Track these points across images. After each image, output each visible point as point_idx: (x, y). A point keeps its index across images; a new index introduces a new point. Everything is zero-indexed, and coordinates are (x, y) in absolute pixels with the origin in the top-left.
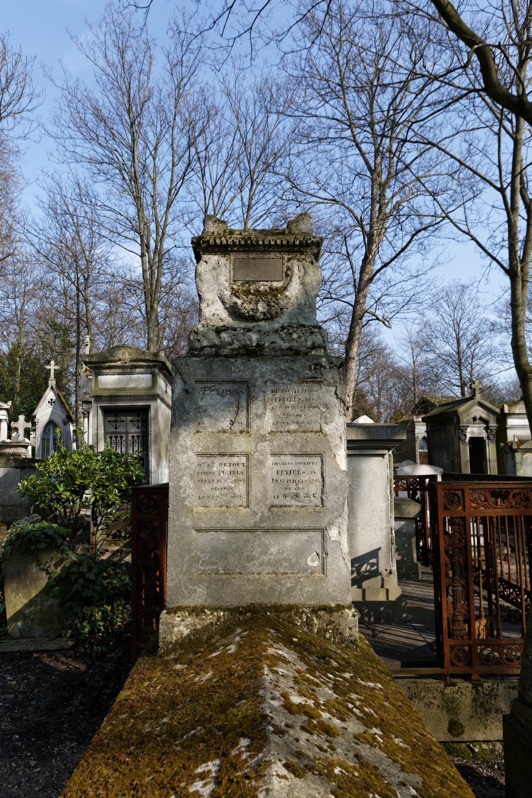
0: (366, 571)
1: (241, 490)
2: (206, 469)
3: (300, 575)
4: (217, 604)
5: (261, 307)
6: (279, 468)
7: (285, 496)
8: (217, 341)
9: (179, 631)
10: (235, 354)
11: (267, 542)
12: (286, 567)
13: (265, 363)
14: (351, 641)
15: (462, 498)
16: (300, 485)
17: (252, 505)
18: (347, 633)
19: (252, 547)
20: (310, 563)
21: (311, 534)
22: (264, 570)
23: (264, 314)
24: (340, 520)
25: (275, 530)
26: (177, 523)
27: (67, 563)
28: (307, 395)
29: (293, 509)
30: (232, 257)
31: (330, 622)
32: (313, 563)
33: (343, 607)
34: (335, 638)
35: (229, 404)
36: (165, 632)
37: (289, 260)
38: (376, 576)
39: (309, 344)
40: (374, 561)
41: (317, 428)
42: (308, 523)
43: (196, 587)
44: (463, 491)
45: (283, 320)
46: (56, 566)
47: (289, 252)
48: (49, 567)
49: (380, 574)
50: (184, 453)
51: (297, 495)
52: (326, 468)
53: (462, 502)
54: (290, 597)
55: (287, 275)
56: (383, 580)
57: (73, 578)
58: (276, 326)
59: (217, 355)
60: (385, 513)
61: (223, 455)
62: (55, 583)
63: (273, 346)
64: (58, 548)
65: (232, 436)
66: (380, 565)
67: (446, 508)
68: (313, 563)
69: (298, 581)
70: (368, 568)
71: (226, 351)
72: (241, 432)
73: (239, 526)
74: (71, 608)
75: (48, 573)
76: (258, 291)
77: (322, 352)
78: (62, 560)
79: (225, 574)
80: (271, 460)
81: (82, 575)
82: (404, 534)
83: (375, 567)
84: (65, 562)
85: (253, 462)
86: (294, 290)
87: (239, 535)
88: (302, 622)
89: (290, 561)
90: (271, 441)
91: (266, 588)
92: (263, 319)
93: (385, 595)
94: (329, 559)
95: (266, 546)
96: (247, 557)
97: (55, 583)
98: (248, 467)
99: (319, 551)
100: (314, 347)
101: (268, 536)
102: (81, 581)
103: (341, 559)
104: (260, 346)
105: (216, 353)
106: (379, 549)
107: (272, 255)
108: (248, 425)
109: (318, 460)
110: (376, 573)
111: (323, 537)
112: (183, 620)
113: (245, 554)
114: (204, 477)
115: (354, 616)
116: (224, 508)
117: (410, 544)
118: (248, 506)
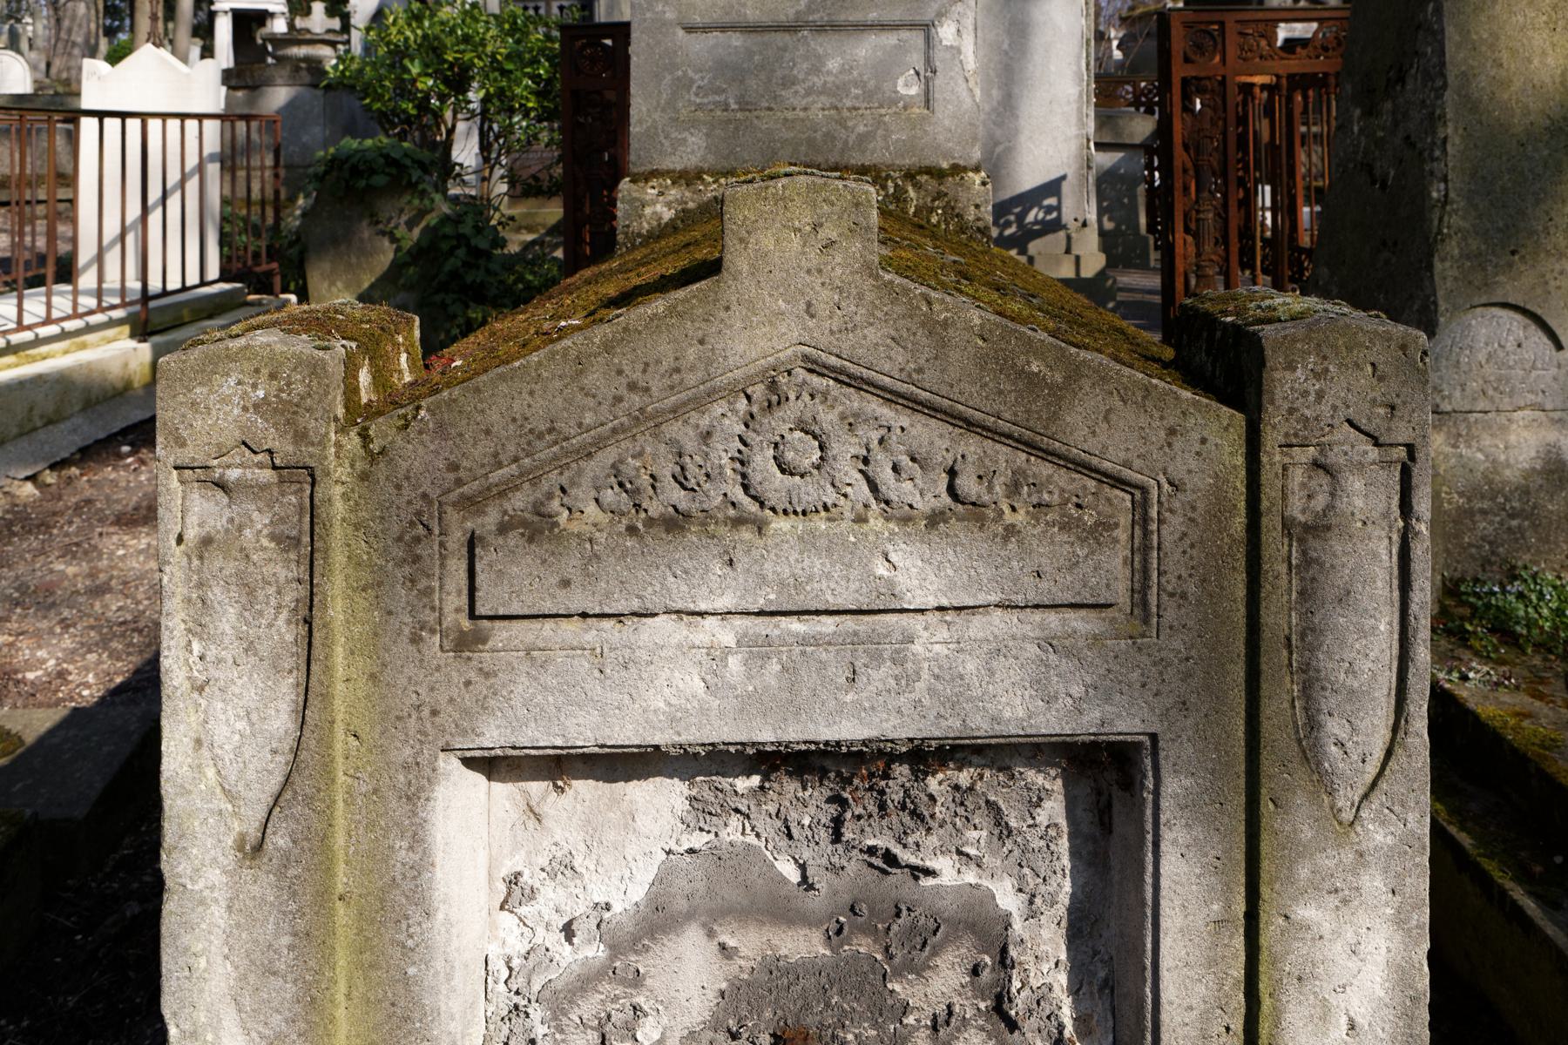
0: (1036, 222)
3: (883, 111)
9: (655, 213)
11: (821, 51)
12: (857, 97)
14: (979, 229)
15: (1219, 40)
18: (971, 214)
19: (793, 60)
20: (902, 90)
21: (905, 34)
22: (814, 102)
25: (835, 27)
26: (648, 15)
27: (431, 219)
31: (939, 195)
32: (908, 87)
33: (965, 169)
34: (947, 224)
36: (627, 216)
38: (1055, 231)
40: (1052, 201)
42: (898, 13)
43: (686, 134)
44: (1222, 24)
46: (410, 225)
48: (396, 227)
49: (1065, 227)
53: (1220, 47)
54: (863, 152)
56: (1069, 238)
57: (445, 246)
60: (1075, 106)
62: (408, 259)
64: (412, 186)
66: (1064, 210)
67: (1187, 60)
68: (908, 87)
69: (879, 122)
70: (1041, 215)
73: (766, 20)
74: (444, 306)
75: (394, 239)
78: (422, 213)
79: (741, 110)
81: (461, 238)
82: (1122, 178)
83: (1054, 215)
84: (428, 217)
87: (767, 37)
88: (887, 195)
89: (863, 85)
91: (819, 135)
93: (1073, 268)
94: (939, 81)
95: (819, 57)
96: (783, 78)
97: (408, 259)
99: (920, 67)
101: (821, 38)
102: (461, 252)
103: (961, 81)
106: (1064, 177)
110: (1056, 226)
112: (661, 194)
113: (779, 73)
115: (984, 184)
117: (1133, 198)
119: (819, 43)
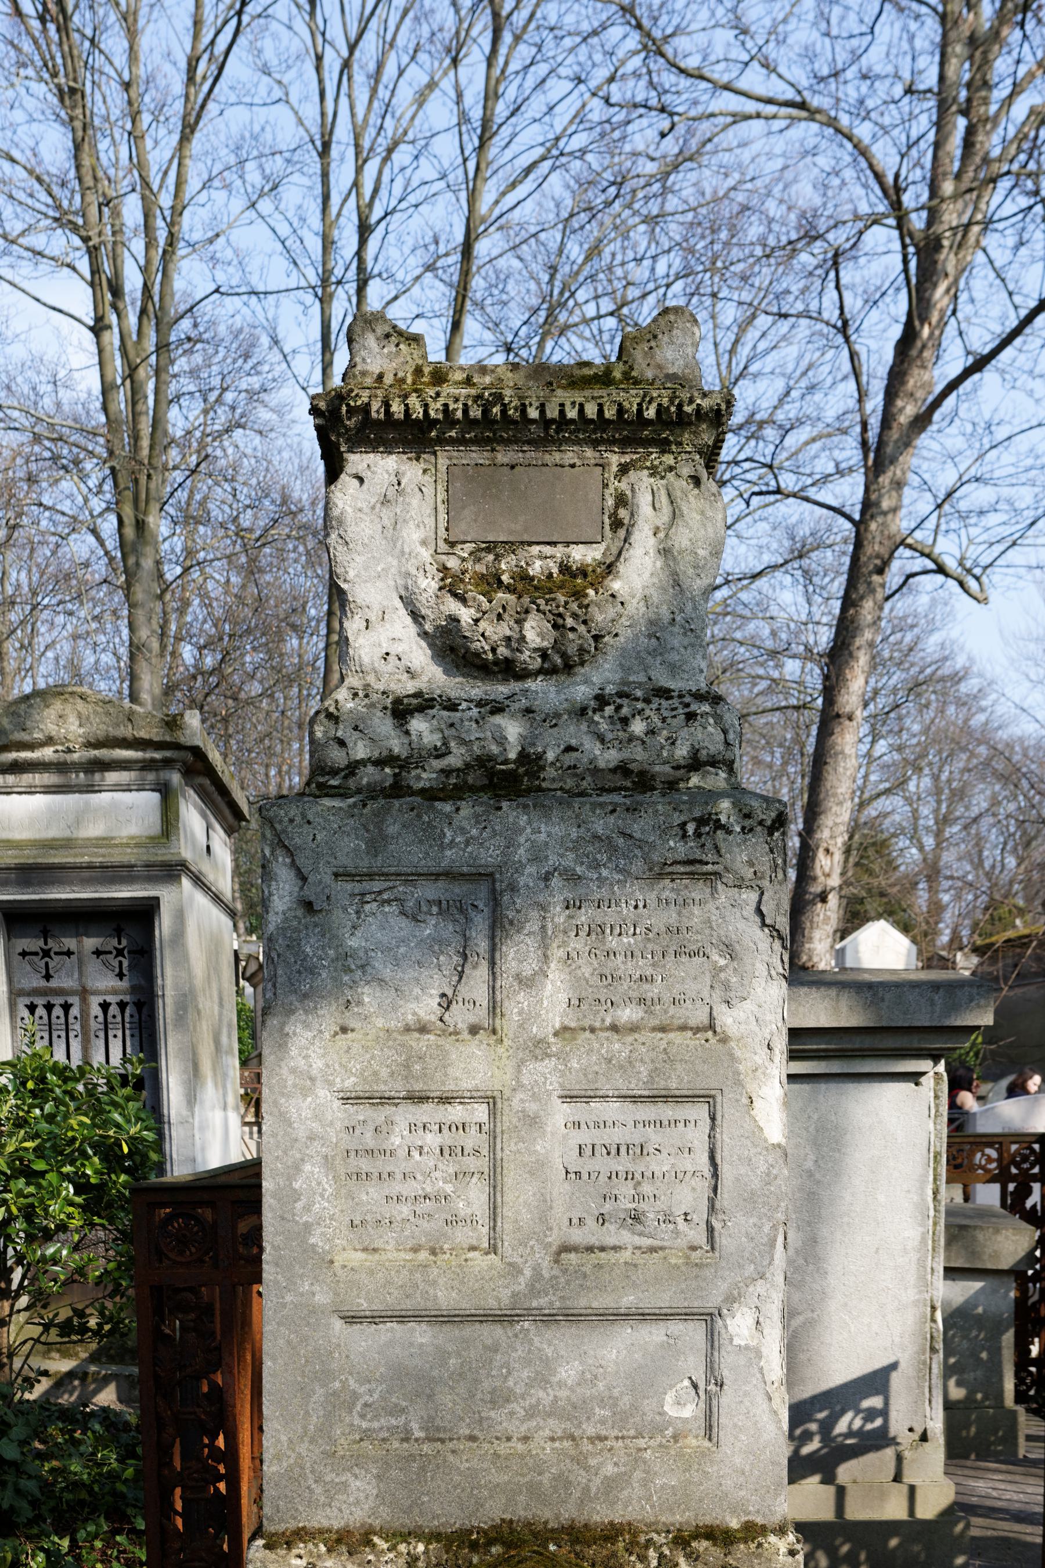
1: (473, 1199)
2: (369, 1140)
3: (642, 1443)
4: (407, 1522)
5: (535, 632)
6: (585, 1137)
7: (602, 1219)
8: (397, 745)
10: (453, 789)
11: (549, 1352)
12: (603, 1422)
13: (548, 817)
16: (647, 1189)
17: (506, 1247)
19: (507, 1365)
20: (671, 1410)
21: (676, 1327)
22: (539, 1428)
23: (544, 655)
24: (760, 1287)
25: (572, 1317)
26: (288, 1298)
28: (671, 917)
29: (626, 1255)
30: (443, 462)
32: (681, 1408)
33: (763, 1530)
35: (436, 945)
37: (624, 470)
39: (682, 752)
41: (700, 1017)
42: (666, 1296)
43: (347, 1476)
45: (601, 674)
47: (625, 443)
50: (305, 1092)
51: (636, 1218)
52: (725, 1138)
54: (613, 1504)
55: (617, 524)
58: (581, 692)
59: (397, 790)
61: (419, 1099)
63: (569, 759)
65: (447, 1043)
69: (636, 1458)
71: (425, 777)
72: (474, 1030)
73: (467, 1305)
76: (523, 577)
77: (718, 779)
79: (429, 1439)
80: (561, 1113)
85: (507, 1119)
86: (638, 576)
87: (468, 1331)
89: (613, 1402)
90: (562, 1057)
92: (540, 671)
94: (727, 1399)
95: (546, 1361)
96: (493, 1392)
98: (493, 1136)
100: (695, 763)
101: (550, 1333)
103: (760, 1399)
104: (530, 760)
105: (397, 784)
107: (569, 455)
108: (494, 1008)
109: (700, 1112)
111: (711, 1335)
113: (486, 1385)
114: (364, 1164)
115: (792, 1553)
116: (423, 1255)
118: (493, 1249)
119: (551, 1342)
